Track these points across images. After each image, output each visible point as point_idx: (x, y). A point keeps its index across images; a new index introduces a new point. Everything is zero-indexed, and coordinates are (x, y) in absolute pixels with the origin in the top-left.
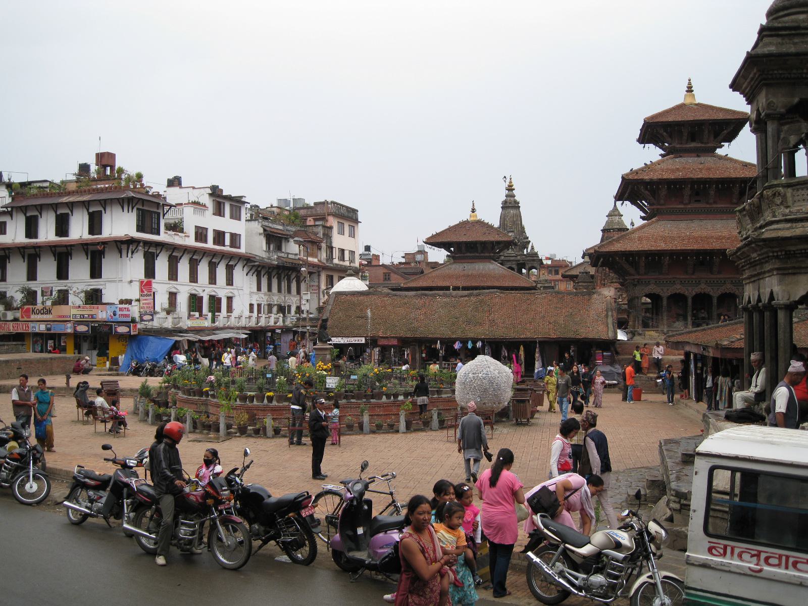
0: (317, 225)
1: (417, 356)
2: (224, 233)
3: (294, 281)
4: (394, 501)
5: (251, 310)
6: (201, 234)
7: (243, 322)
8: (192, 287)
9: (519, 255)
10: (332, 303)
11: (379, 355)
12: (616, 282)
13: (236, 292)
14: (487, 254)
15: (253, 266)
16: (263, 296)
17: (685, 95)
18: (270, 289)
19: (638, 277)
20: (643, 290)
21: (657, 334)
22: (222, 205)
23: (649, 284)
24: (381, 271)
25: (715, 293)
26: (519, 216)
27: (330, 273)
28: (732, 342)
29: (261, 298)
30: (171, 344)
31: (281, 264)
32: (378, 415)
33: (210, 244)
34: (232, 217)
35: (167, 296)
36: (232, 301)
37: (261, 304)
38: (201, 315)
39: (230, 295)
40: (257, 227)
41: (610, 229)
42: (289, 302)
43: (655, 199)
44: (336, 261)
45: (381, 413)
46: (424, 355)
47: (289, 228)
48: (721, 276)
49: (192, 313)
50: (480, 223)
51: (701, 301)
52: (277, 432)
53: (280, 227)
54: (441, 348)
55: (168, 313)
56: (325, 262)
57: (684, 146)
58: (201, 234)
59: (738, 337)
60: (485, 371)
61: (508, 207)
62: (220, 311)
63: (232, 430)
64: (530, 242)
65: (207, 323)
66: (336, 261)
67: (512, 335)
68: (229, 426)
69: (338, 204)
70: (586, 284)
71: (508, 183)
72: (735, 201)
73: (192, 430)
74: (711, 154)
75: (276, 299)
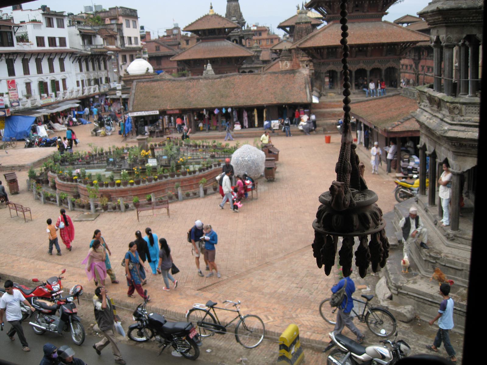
2: (54, 38)
4: (240, 316)
5: (78, 85)
6: (40, 41)
7: (74, 95)
12: (305, 56)
13: (67, 75)
14: (222, 36)
15: (76, 57)
16: (84, 75)
18: (88, 69)
21: (335, 95)
23: (329, 64)
24: (154, 45)
25: (368, 68)
26: (238, 6)
27: (124, 54)
28: (394, 127)
29: (84, 76)
30: (33, 120)
31: (93, 54)
32: (185, 186)
33: (47, 47)
34: (58, 27)
35: (25, 85)
39: (64, 78)
40: (75, 30)
42: (100, 76)
44: (127, 45)
45: (187, 184)
46: (196, 118)
47: (95, 28)
49: (42, 95)
50: (216, 16)
52: (127, 207)
53: (89, 28)
54: (207, 113)
55: (28, 98)
56: (120, 47)
58: (40, 41)
59: (396, 123)
60: (249, 156)
62: (58, 90)
64: (245, 23)
65: (52, 100)
66: (127, 45)
67: (249, 102)
68: (96, 206)
69: (124, 8)
72: (379, 10)
73: (72, 208)
75: (93, 75)
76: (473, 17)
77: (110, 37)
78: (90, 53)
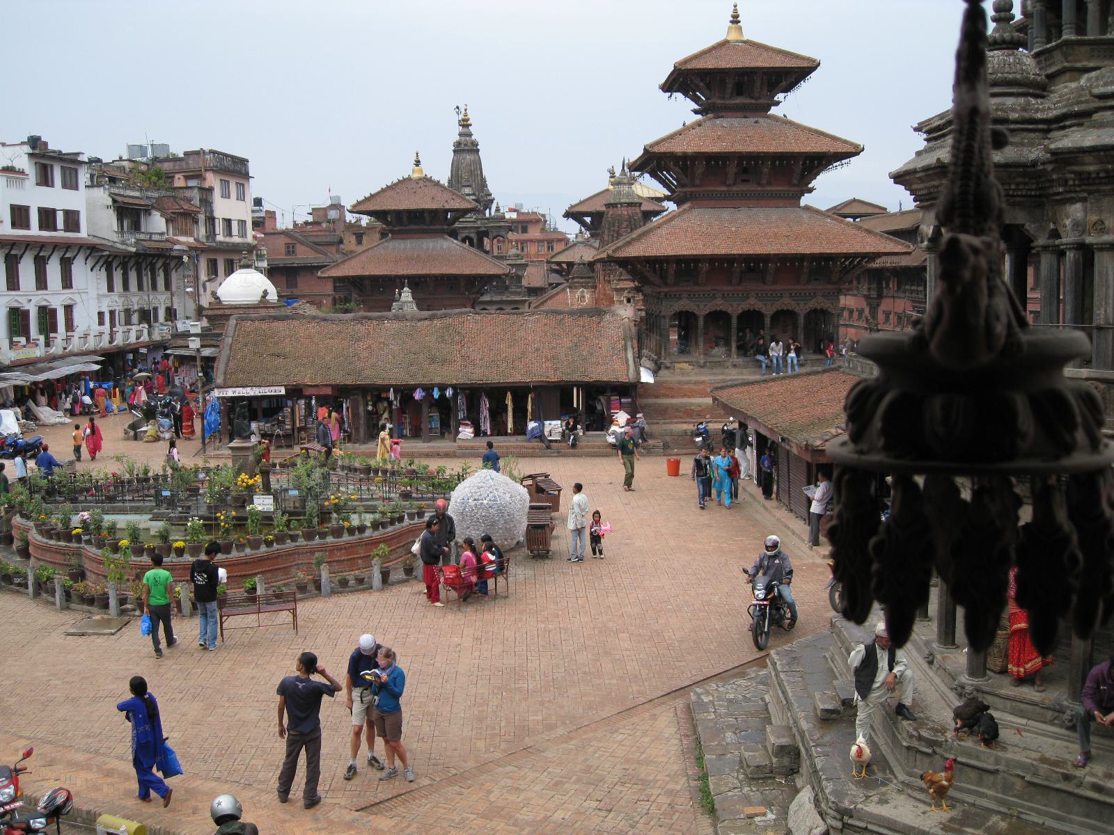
0: (191, 188)
1: (361, 409)
2: (54, 211)
3: (161, 271)
5: (101, 323)
7: (91, 344)
8: (12, 297)
9: (480, 219)
10: (232, 334)
12: (625, 280)
13: (77, 298)
14: (438, 227)
16: (117, 299)
17: (730, 28)
18: (126, 287)
19: (666, 290)
20: (671, 306)
21: (692, 367)
23: (680, 298)
24: (281, 242)
25: (768, 310)
27: (212, 256)
28: (826, 441)
29: (115, 302)
31: (141, 252)
33: (34, 230)
34: (65, 186)
36: (72, 311)
37: (115, 310)
38: (28, 340)
39: (68, 302)
40: (102, 196)
41: (616, 204)
42: (155, 303)
43: (687, 176)
44: (220, 238)
46: (370, 408)
47: (149, 194)
48: (777, 287)
49: (15, 339)
50: (427, 180)
51: (751, 319)
53: (137, 194)
54: (396, 398)
57: (727, 102)
59: (833, 431)
61: (463, 151)
62: (55, 331)
63: (129, 606)
64: (492, 201)
65: (38, 352)
66: (220, 238)
67: (495, 377)
68: (122, 601)
69: (219, 153)
70: (583, 280)
72: (795, 181)
73: (65, 604)
75: (137, 300)
76: (1017, 184)
77: (182, 218)
78: (134, 250)
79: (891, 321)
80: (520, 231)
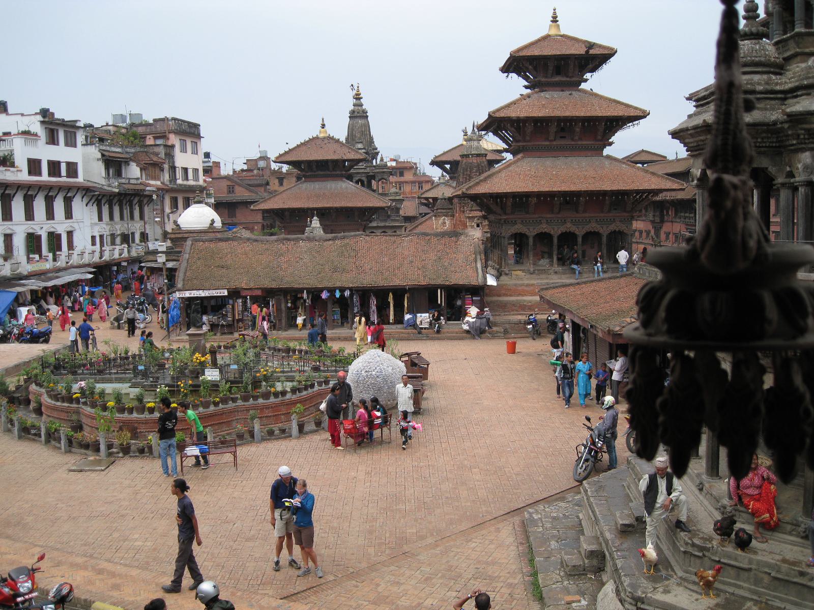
0: (158, 145)
1: (283, 306)
2: (59, 163)
3: (137, 205)
5: (94, 244)
6: (34, 166)
7: (86, 259)
9: (369, 167)
10: (188, 251)
11: (242, 306)
12: (475, 210)
13: (76, 226)
15: (93, 196)
16: (105, 226)
17: (550, 26)
18: (111, 218)
20: (509, 229)
21: (524, 274)
22: (55, 132)
23: (515, 223)
24: (224, 184)
25: (580, 232)
26: (367, 126)
27: (174, 195)
28: (623, 327)
29: (103, 228)
30: (12, 296)
33: (45, 177)
34: (67, 144)
37: (103, 235)
38: (41, 256)
39: (70, 229)
40: (94, 152)
41: (468, 155)
42: (132, 229)
43: (520, 134)
44: (180, 182)
45: (270, 414)
46: (289, 305)
47: (128, 150)
48: (587, 215)
49: (31, 256)
50: (330, 139)
51: (568, 239)
54: (308, 297)
55: (6, 259)
56: (168, 183)
57: (549, 80)
58: (34, 166)
59: (628, 320)
60: (378, 368)
61: (356, 117)
62: (60, 250)
63: (114, 450)
64: (377, 153)
65: (48, 265)
66: (180, 182)
68: (110, 446)
69: (178, 120)
70: (445, 211)
71: (355, 92)
72: (599, 137)
73: (68, 448)
74: (575, 88)
75: (119, 228)
76: (762, 138)
77: (152, 167)
78: (117, 190)
79: (671, 239)
80: (398, 176)
